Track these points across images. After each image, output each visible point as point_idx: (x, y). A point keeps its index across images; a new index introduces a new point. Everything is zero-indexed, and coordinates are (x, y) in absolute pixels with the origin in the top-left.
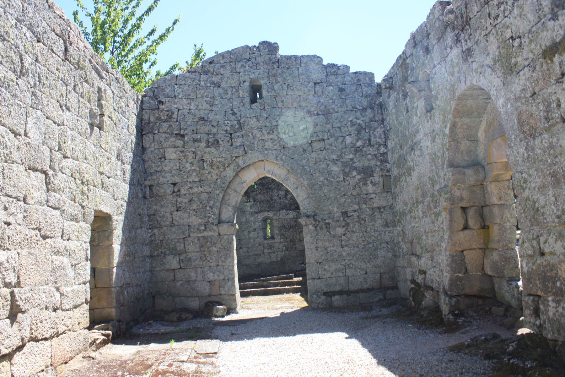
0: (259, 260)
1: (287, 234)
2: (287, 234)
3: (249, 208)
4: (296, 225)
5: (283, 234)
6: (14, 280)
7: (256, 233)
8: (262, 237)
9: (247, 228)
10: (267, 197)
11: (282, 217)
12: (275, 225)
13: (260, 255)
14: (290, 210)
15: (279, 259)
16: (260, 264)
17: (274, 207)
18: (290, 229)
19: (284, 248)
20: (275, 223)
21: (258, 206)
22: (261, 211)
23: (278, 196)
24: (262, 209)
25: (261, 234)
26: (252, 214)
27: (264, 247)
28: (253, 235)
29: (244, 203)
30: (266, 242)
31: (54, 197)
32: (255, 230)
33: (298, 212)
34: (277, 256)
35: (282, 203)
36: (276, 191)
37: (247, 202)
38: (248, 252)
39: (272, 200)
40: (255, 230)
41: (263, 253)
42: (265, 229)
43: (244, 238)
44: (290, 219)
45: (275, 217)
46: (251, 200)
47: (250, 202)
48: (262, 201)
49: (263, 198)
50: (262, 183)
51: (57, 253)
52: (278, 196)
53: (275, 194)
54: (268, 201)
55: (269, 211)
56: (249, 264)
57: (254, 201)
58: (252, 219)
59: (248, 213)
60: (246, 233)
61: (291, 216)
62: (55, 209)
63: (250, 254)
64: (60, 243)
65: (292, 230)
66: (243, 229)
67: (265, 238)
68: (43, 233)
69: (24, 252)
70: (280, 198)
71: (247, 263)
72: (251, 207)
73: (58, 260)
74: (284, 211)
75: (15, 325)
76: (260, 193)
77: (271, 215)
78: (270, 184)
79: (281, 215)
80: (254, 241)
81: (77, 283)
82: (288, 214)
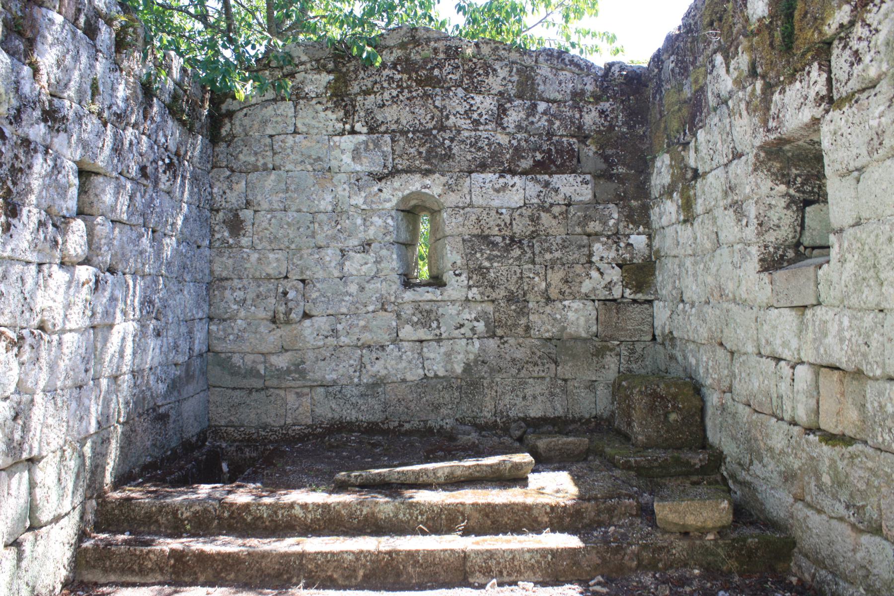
0: (378, 368)
1: (497, 271)
2: (497, 271)
3: (347, 158)
4: (533, 235)
5: (481, 271)
7: (371, 257)
8: (395, 277)
9: (334, 238)
10: (424, 117)
11: (478, 200)
12: (448, 230)
13: (383, 347)
14: (513, 173)
15: (459, 369)
16: (378, 383)
17: (449, 156)
18: (508, 248)
19: (481, 326)
20: (451, 223)
21: (387, 149)
22: (394, 172)
23: (467, 114)
24: (402, 164)
25: (392, 263)
26: (357, 182)
27: (398, 316)
28: (357, 264)
29: (330, 136)
30: (409, 295)
32: (366, 246)
33: (547, 184)
34: (448, 355)
35: (483, 144)
36: (460, 92)
37: (342, 134)
38: (335, 332)
39: (442, 128)
40: (366, 246)
41: (396, 340)
42: (408, 245)
43: (320, 274)
44: (513, 210)
45: (452, 199)
46: (358, 127)
47: (353, 132)
48: (404, 133)
49: (406, 119)
50: (407, 59)
52: (467, 114)
53: (455, 103)
54: (427, 132)
55: (427, 173)
56: (335, 383)
57: (372, 130)
58: (359, 200)
59: (343, 177)
60: (330, 255)
61: (515, 198)
63: (344, 340)
65: (516, 252)
66: (320, 239)
67: (408, 282)
70: (477, 123)
71: (330, 377)
72: (356, 155)
74: (489, 176)
76: (394, 100)
77: (436, 190)
78: (440, 66)
79: (476, 191)
80: (362, 289)
82: (505, 187)
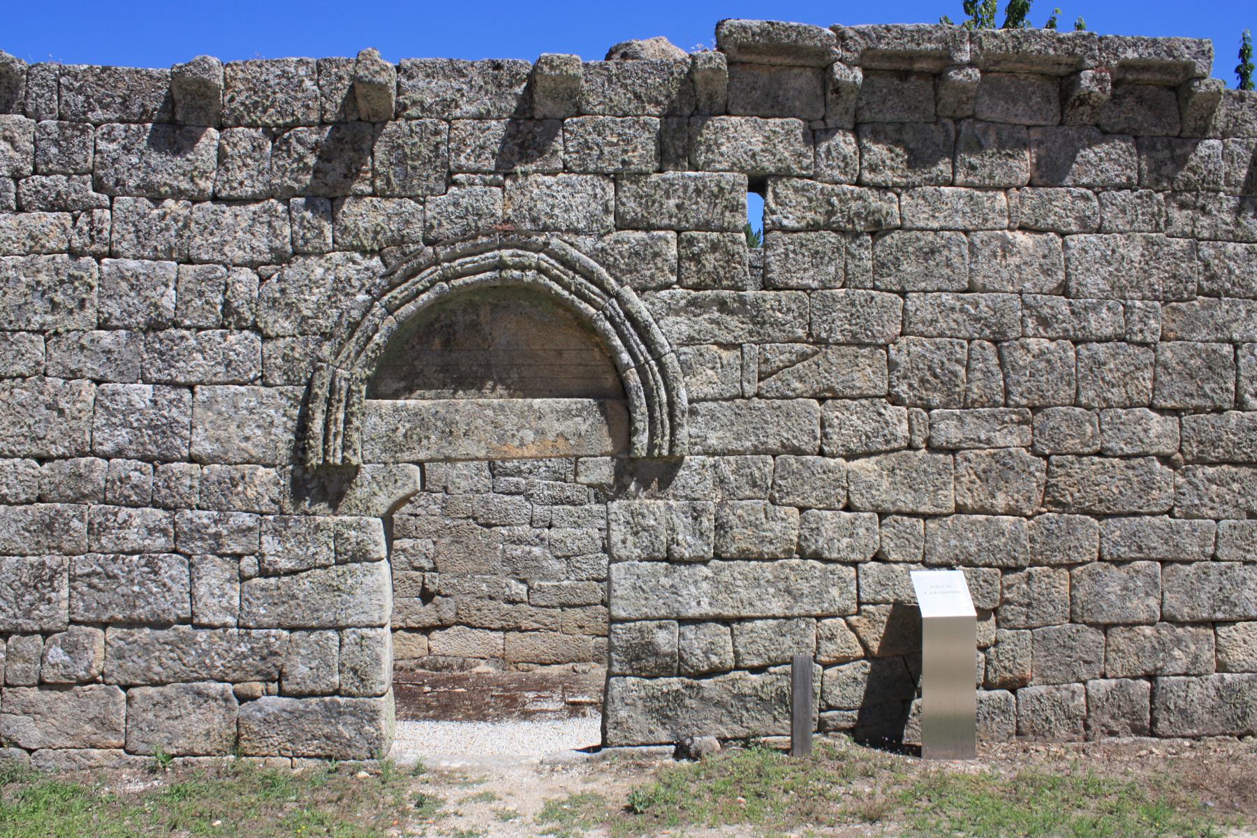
6: (427, 564)
31: (503, 482)
51: (519, 541)
62: (511, 494)
64: (524, 530)
68: (481, 520)
69: (447, 540)
73: (518, 551)
75: (428, 606)
81: (572, 578)
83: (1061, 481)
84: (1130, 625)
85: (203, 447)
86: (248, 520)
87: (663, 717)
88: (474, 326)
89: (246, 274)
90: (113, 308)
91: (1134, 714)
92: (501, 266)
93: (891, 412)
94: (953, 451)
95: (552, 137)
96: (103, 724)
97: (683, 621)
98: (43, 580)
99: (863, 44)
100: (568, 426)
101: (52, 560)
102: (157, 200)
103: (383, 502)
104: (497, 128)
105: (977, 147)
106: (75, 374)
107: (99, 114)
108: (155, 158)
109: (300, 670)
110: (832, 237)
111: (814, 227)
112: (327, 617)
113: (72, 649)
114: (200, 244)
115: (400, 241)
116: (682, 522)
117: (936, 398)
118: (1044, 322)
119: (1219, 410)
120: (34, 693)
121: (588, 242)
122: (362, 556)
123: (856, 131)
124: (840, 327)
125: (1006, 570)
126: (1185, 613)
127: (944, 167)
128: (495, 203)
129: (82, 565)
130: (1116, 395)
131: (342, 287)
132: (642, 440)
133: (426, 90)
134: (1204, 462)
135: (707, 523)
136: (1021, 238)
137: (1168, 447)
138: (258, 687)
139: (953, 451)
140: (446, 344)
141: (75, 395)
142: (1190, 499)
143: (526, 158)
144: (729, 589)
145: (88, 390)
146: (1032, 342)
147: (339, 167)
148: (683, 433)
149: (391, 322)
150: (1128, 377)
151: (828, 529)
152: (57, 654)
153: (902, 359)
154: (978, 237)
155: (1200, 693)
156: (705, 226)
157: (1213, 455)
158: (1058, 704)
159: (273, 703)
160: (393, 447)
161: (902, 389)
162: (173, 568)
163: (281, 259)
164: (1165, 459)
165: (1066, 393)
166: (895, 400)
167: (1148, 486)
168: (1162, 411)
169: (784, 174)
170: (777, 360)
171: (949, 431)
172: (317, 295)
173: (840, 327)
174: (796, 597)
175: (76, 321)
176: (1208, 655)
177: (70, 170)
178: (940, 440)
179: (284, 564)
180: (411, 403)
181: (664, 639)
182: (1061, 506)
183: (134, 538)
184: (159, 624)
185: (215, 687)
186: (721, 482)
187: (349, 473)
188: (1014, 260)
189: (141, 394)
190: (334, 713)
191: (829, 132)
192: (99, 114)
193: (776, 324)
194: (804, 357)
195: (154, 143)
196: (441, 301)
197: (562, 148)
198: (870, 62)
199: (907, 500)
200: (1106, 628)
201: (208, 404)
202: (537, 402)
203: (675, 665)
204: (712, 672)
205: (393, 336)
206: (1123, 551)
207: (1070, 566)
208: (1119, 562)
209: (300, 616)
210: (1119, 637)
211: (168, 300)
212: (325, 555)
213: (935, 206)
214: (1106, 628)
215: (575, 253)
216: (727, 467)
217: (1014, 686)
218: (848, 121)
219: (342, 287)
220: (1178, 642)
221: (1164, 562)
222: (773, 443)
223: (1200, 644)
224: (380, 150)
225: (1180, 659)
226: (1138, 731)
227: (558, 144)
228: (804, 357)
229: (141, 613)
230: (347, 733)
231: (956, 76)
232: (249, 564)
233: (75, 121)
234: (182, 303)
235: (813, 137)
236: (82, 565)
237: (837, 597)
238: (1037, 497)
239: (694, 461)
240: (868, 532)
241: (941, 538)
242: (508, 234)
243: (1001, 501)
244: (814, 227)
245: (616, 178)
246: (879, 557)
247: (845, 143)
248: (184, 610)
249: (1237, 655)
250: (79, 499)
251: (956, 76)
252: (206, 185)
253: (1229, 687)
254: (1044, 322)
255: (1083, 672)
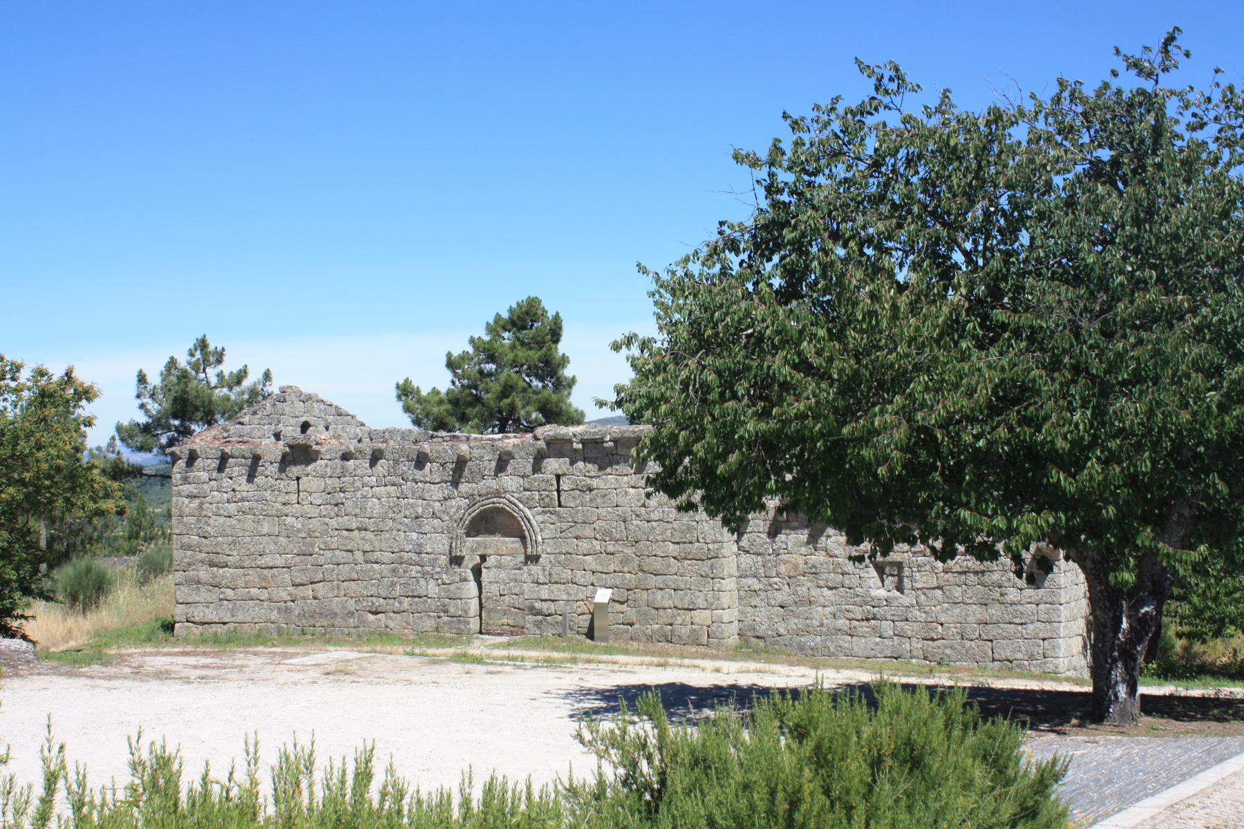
83: (643, 564)
84: (665, 609)
85: (430, 550)
86: (439, 570)
87: (539, 628)
88: (492, 518)
89: (437, 504)
90: (407, 513)
91: (666, 637)
92: (494, 503)
93: (595, 542)
94: (613, 554)
95: (507, 465)
96: (408, 623)
97: (542, 600)
98: (393, 584)
99: (579, 437)
100: (511, 546)
101: (395, 579)
102: (417, 483)
103: (471, 565)
104: (494, 464)
105: (618, 463)
106: (399, 530)
107: (402, 459)
108: (416, 472)
109: (452, 610)
110: (578, 492)
111: (573, 490)
112: (458, 596)
113: (400, 603)
114: (427, 496)
115: (472, 495)
116: (540, 573)
117: (607, 539)
118: (637, 516)
119: (691, 543)
120: (392, 614)
121: (516, 495)
122: (465, 580)
123: (584, 461)
124: (580, 518)
125: (628, 590)
126: (680, 606)
127: (609, 470)
128: (493, 484)
129: (402, 581)
130: (659, 538)
131: (459, 508)
132: (529, 550)
133: (476, 453)
134: (686, 559)
135: (547, 573)
136: (631, 490)
137: (675, 554)
138: (442, 614)
139: (613, 554)
140: (486, 522)
141: (399, 536)
142: (682, 570)
143: (501, 472)
144: (552, 592)
145: (402, 535)
146: (634, 522)
147: (457, 475)
148: (540, 548)
149: (470, 518)
150: (663, 533)
151: (578, 576)
152: (397, 604)
153: (597, 528)
154: (618, 491)
155: (684, 631)
156: (544, 490)
157: (690, 557)
158: (643, 632)
159: (446, 619)
160: (473, 551)
161: (598, 536)
162: (422, 582)
163: (445, 499)
164: (675, 558)
165: (644, 537)
166: (596, 539)
167: (669, 566)
168: (674, 543)
169: (564, 475)
170: (564, 528)
171: (611, 549)
172: (453, 510)
173: (580, 518)
174: (570, 595)
175: (399, 515)
176: (688, 619)
177: (396, 474)
178: (608, 551)
179: (448, 582)
180: (476, 539)
181: (538, 605)
182: (645, 572)
183: (414, 574)
184: (420, 597)
185: (432, 614)
186: (551, 562)
187: (462, 558)
188: (628, 497)
189: (414, 536)
190: (459, 622)
191: (576, 462)
192: (402, 459)
193: (564, 518)
194: (571, 527)
195: (415, 467)
196: (481, 512)
197: (509, 469)
198: (583, 442)
199: (599, 568)
200: (657, 609)
201: (430, 539)
202: (506, 539)
203: (539, 613)
204: (549, 615)
205: (471, 522)
206: (662, 586)
207: (647, 590)
208: (661, 589)
209: (452, 596)
210: (661, 612)
211: (420, 510)
212: (457, 579)
213: (606, 481)
214: (657, 609)
215: (512, 499)
216: (552, 557)
217: (631, 625)
218: (581, 458)
219: (459, 508)
220: (679, 615)
221: (675, 590)
222: (564, 551)
223: (687, 616)
224: (466, 470)
225: (679, 620)
226: (668, 641)
227: (508, 468)
228: (571, 527)
229: (415, 594)
230: (463, 627)
231: (605, 445)
232: (440, 581)
233: (396, 461)
234: (423, 511)
235: (572, 463)
236: (402, 581)
237: (581, 596)
238: (637, 568)
239: (544, 556)
240: (591, 578)
241: (609, 579)
242: (498, 494)
243: (626, 569)
244: (573, 490)
245: (523, 477)
246: (592, 584)
247: (580, 464)
248: (425, 593)
249: (696, 620)
250: (401, 563)
251: (605, 445)
252: (428, 479)
253: (694, 630)
254: (637, 516)
255: (651, 622)
